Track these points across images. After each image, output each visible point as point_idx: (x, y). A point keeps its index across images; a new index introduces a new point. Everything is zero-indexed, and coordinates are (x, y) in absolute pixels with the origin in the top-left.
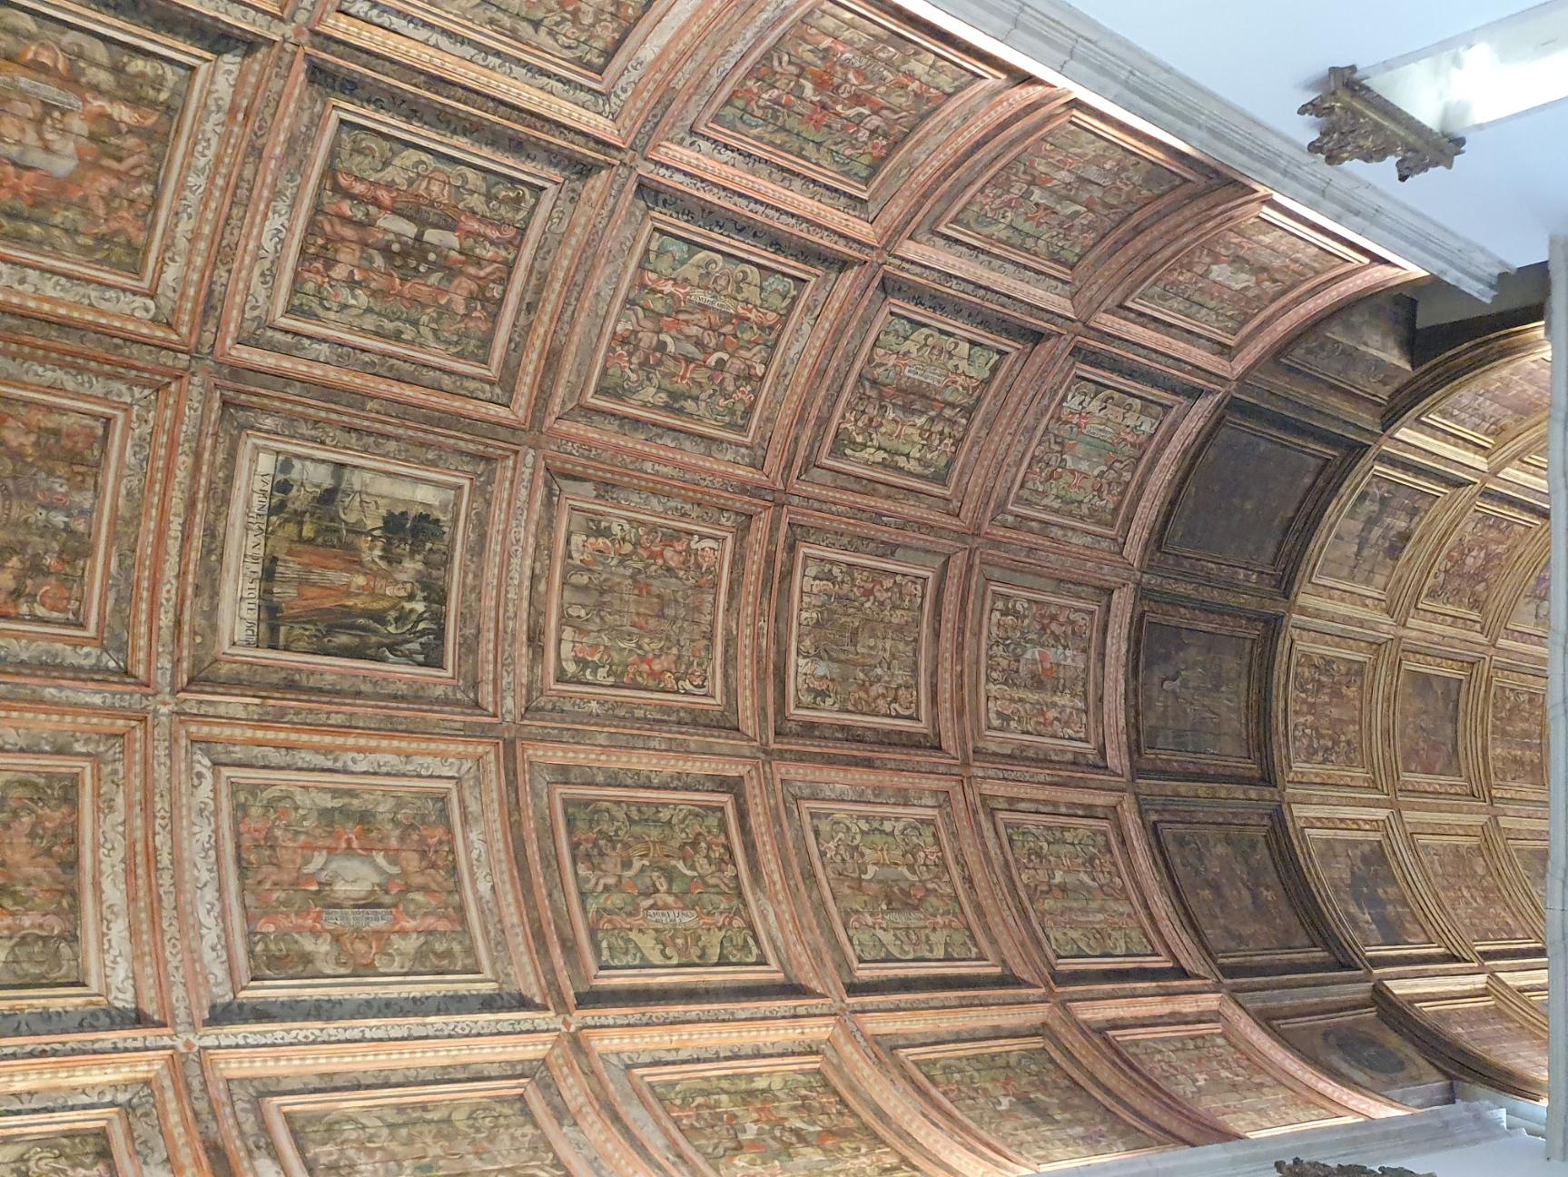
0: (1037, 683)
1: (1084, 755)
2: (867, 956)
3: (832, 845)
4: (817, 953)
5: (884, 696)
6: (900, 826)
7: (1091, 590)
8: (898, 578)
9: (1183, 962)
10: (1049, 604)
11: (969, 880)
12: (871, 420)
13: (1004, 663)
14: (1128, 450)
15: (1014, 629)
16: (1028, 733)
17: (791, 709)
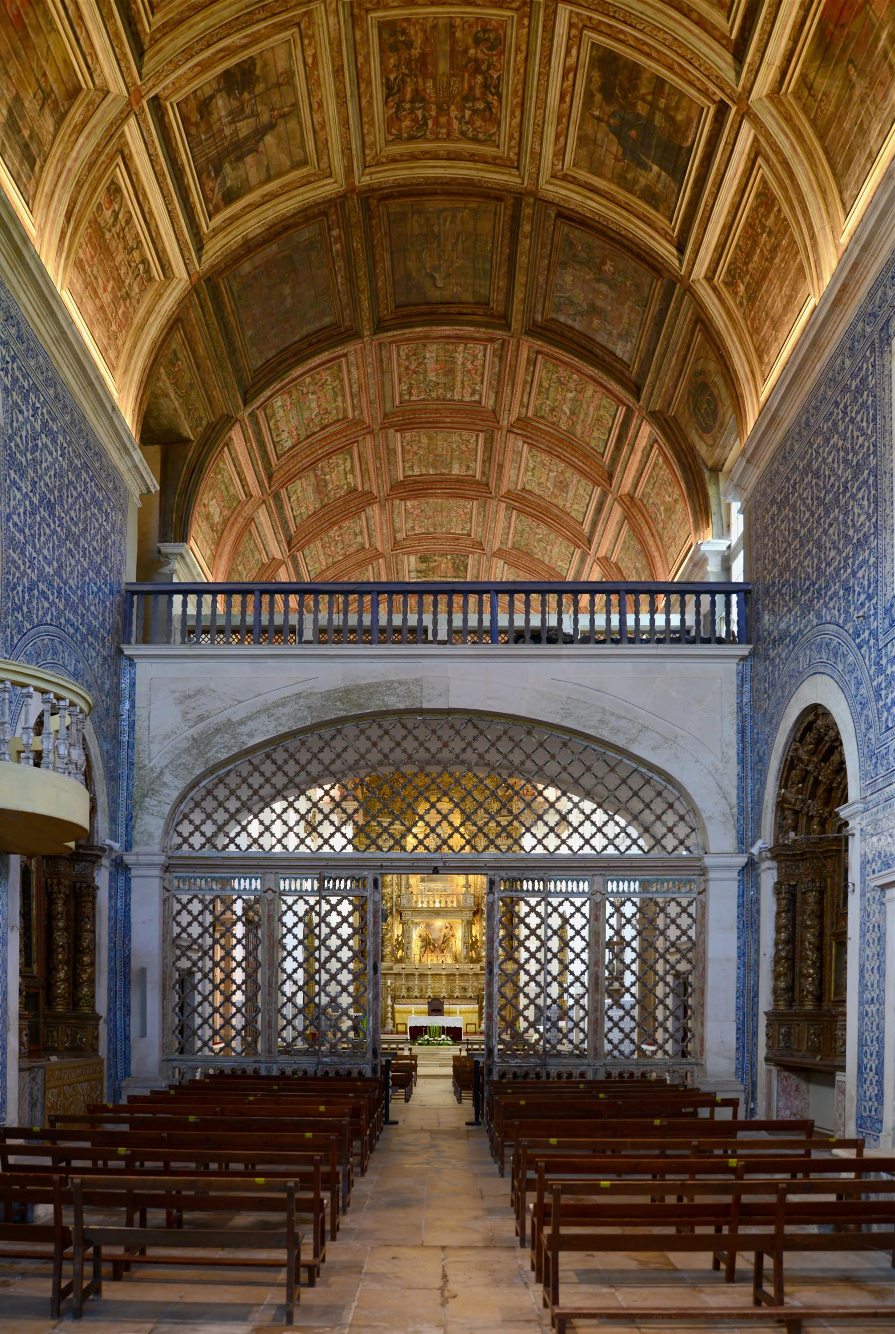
0: (450, 372)
1: (495, 351)
7: (383, 353)
14: (295, 394)
15: (419, 388)
16: (482, 380)
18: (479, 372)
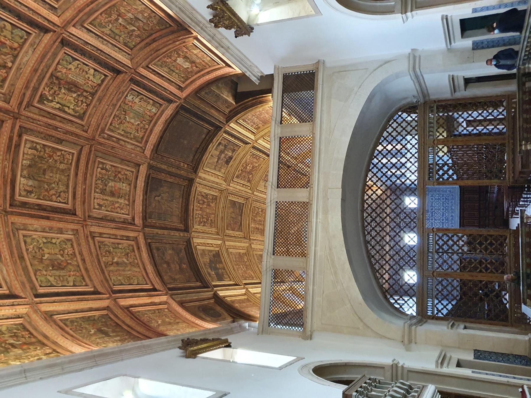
0: (112, 194)
1: (127, 219)
2: (42, 285)
3: (31, 246)
4: (23, 284)
5: (54, 194)
6: (58, 241)
7: (133, 164)
8: (63, 152)
9: (156, 287)
10: (118, 167)
11: (84, 260)
12: (55, 92)
13: (101, 187)
14: (148, 118)
16: (108, 211)
17: (17, 197)
18: (113, 210)
